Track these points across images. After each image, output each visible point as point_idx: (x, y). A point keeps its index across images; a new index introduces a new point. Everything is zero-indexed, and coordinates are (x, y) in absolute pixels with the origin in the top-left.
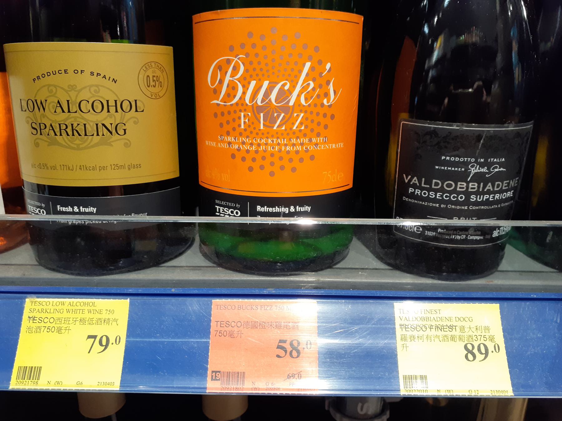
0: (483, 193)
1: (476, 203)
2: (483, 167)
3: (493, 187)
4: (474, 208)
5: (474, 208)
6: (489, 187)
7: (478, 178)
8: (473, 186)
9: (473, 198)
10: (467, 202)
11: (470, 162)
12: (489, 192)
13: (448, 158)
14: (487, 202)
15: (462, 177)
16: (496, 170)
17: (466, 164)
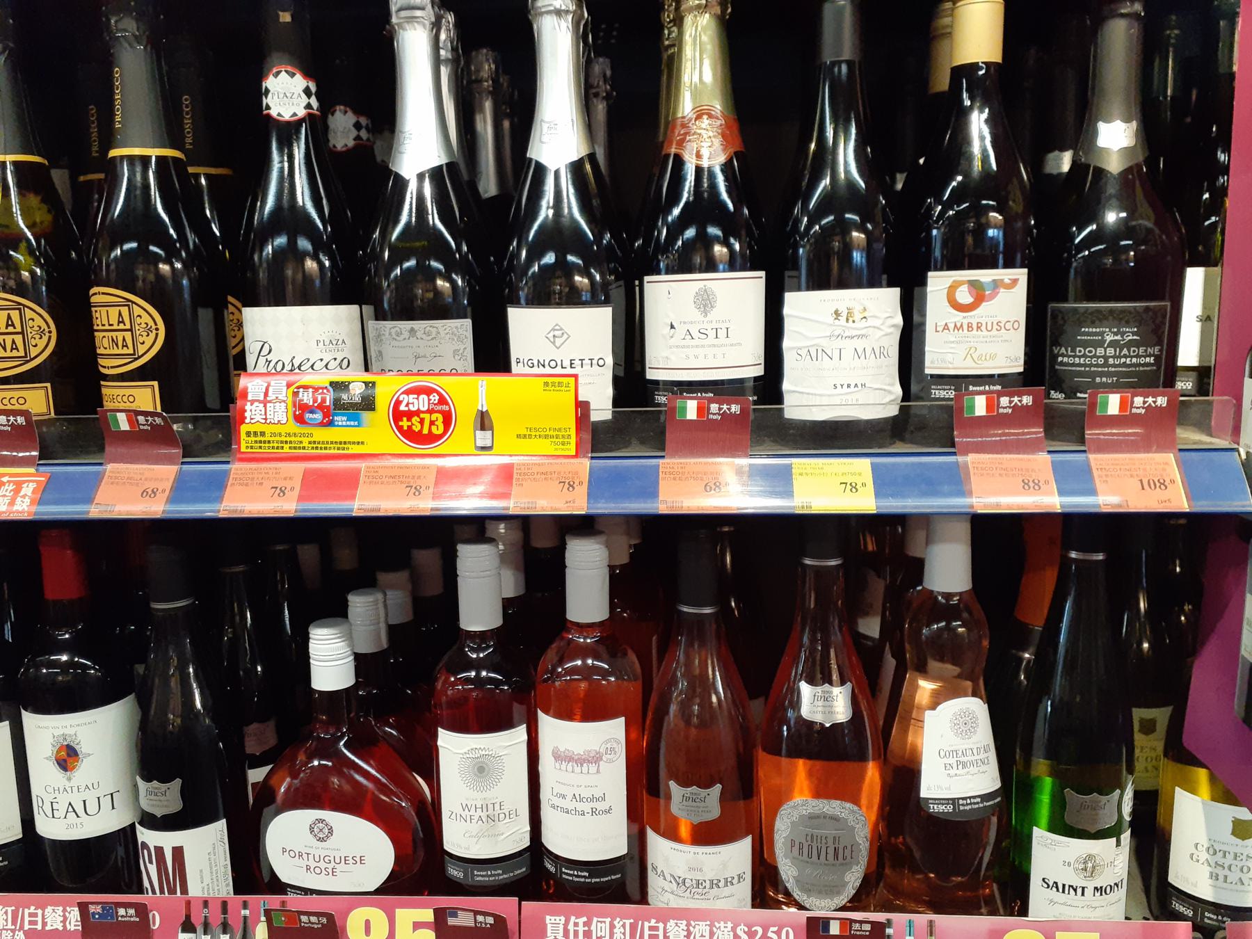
0: (1120, 357)
1: (1114, 366)
2: (1117, 335)
3: (1129, 351)
4: (1113, 369)
5: (1113, 369)
6: (1125, 351)
7: (1113, 344)
8: (1110, 351)
9: (1111, 361)
10: (1106, 365)
11: (1105, 332)
12: (1125, 356)
13: (1087, 330)
14: (1124, 365)
15: (1100, 344)
16: (1130, 338)
17: (1102, 334)
